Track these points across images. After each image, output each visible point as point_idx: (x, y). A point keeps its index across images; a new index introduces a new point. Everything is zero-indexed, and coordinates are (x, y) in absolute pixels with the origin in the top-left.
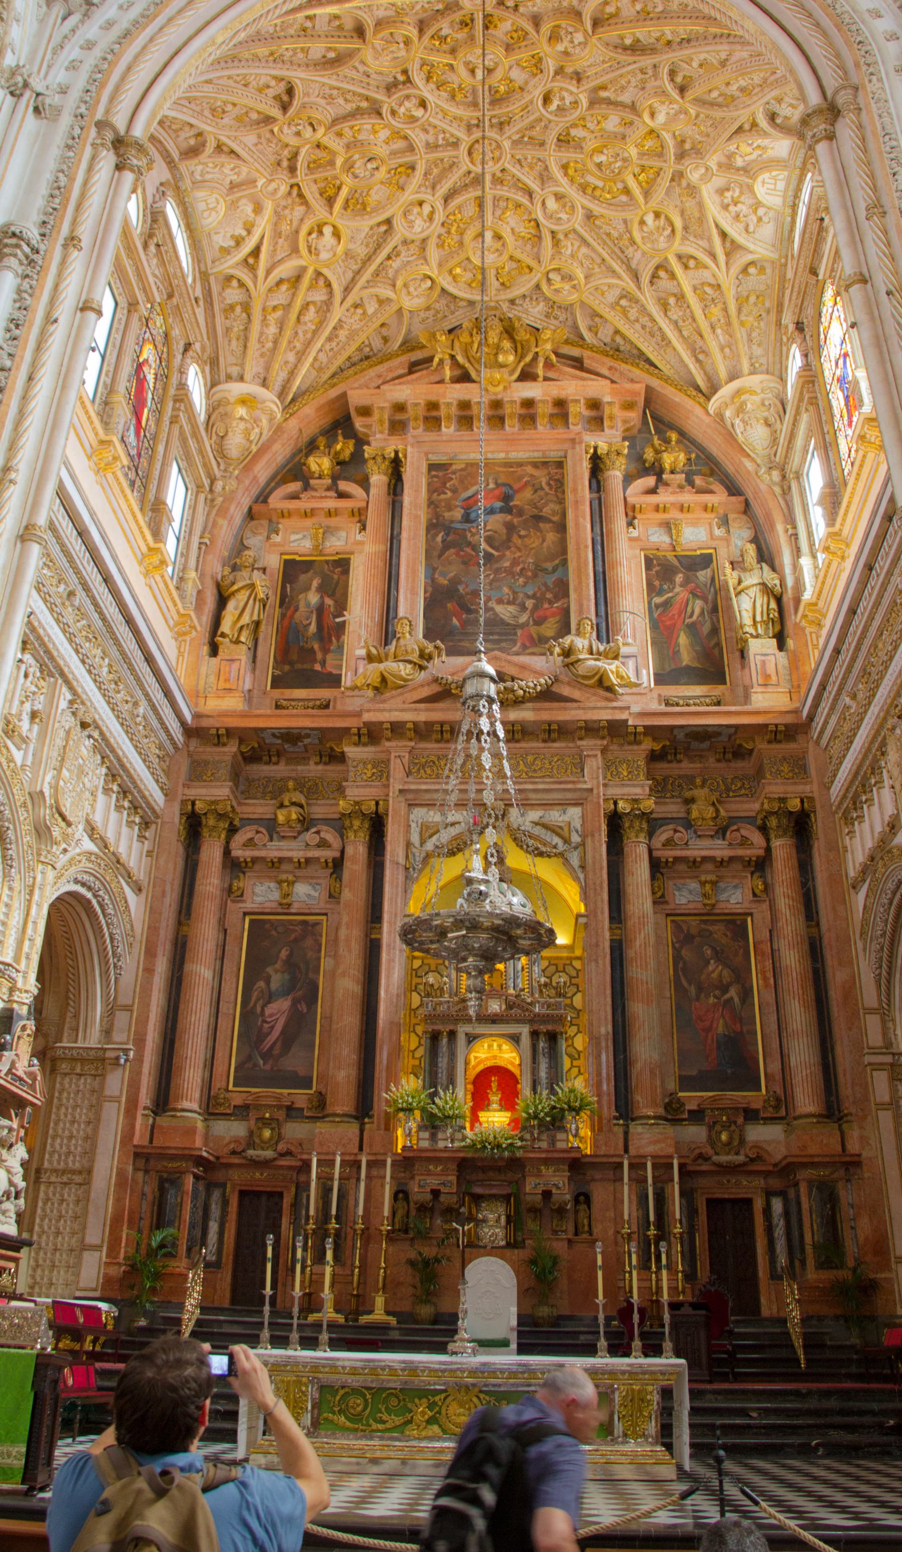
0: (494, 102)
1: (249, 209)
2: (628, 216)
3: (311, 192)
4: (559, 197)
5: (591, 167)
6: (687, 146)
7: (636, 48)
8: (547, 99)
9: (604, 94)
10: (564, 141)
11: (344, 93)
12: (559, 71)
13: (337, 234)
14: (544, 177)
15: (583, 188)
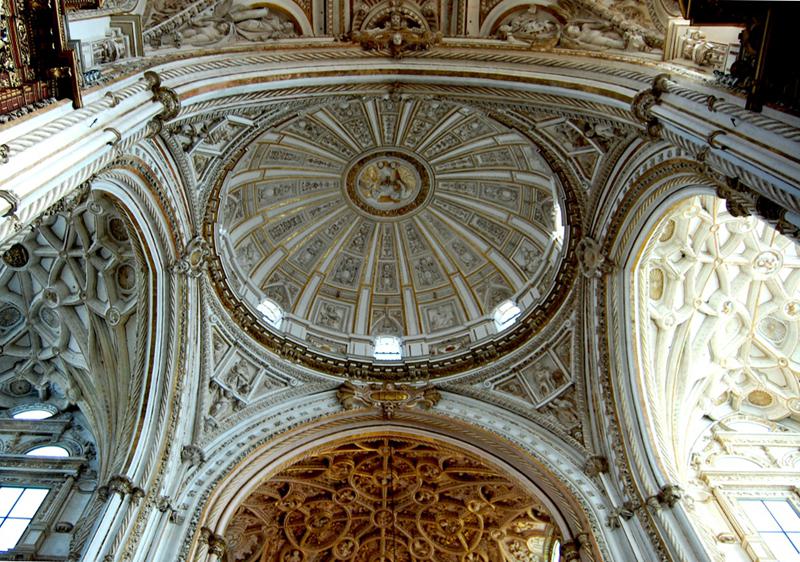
0: (391, 493)
1: (255, 539)
2: (459, 554)
3: (289, 533)
4: (422, 542)
5: (439, 528)
6: (491, 521)
7: (467, 478)
8: (418, 495)
9: (447, 495)
10: (426, 515)
11: (313, 488)
12: (424, 483)
13: (301, 555)
14: (414, 532)
15: (435, 538)
